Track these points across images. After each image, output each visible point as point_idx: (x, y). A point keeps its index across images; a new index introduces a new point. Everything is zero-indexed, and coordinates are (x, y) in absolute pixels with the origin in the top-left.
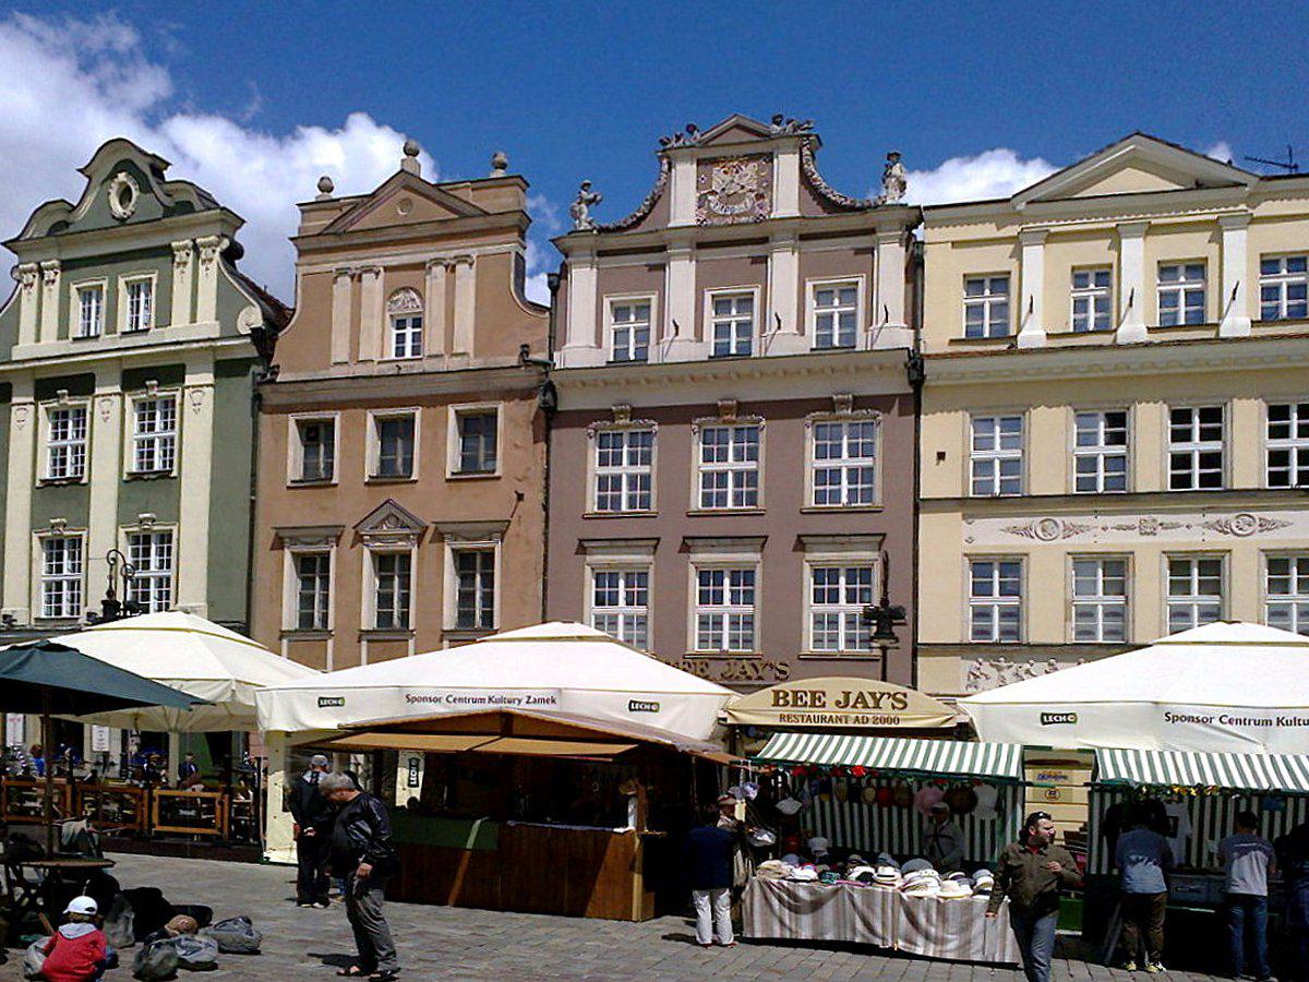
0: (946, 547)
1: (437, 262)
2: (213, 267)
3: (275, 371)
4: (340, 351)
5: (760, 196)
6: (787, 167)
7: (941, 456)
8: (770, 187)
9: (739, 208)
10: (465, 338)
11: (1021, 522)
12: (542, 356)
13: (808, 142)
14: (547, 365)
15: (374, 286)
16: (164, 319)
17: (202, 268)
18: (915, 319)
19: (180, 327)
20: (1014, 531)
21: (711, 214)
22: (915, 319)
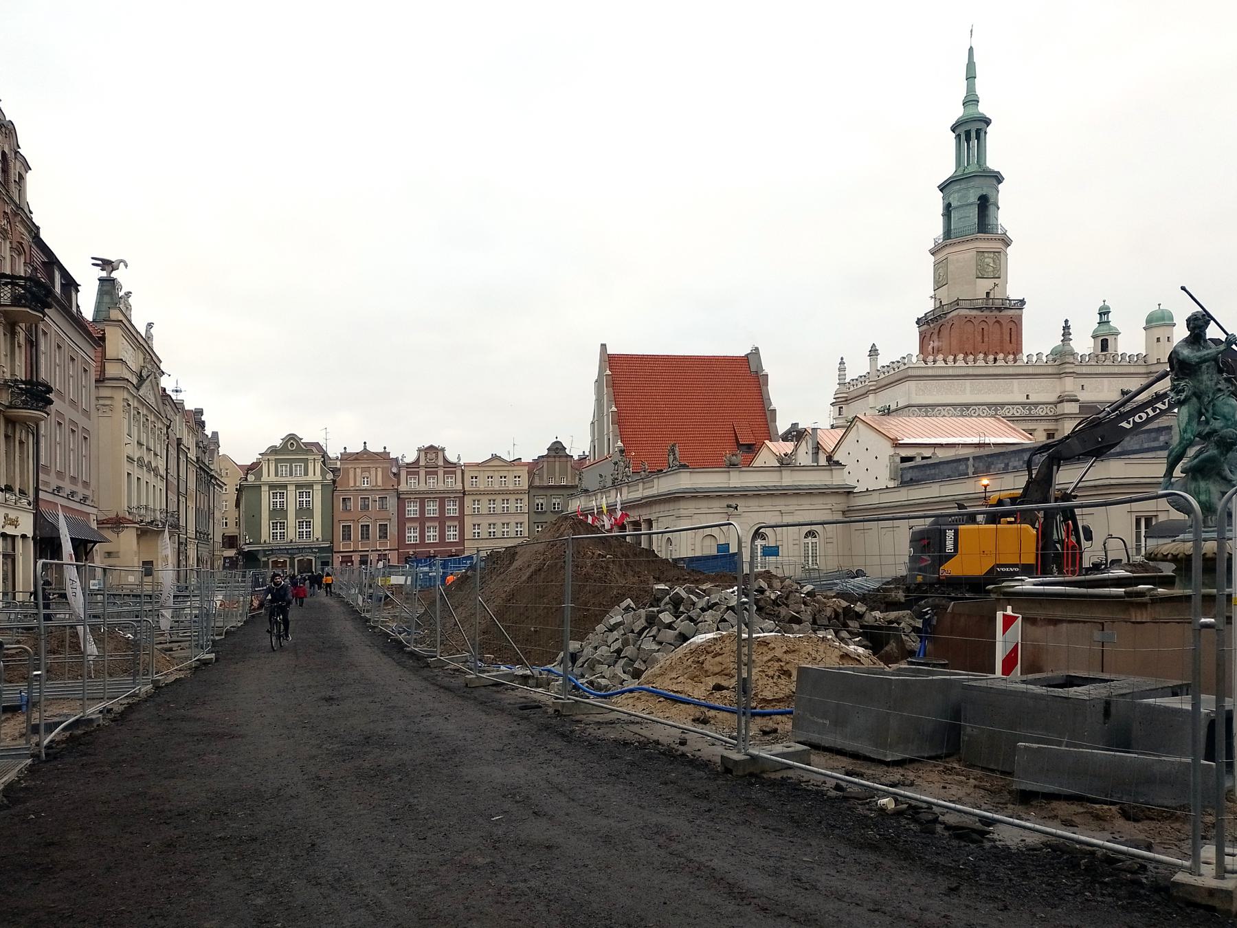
6: (440, 454)
10: (380, 483)
16: (306, 474)
19: (311, 477)
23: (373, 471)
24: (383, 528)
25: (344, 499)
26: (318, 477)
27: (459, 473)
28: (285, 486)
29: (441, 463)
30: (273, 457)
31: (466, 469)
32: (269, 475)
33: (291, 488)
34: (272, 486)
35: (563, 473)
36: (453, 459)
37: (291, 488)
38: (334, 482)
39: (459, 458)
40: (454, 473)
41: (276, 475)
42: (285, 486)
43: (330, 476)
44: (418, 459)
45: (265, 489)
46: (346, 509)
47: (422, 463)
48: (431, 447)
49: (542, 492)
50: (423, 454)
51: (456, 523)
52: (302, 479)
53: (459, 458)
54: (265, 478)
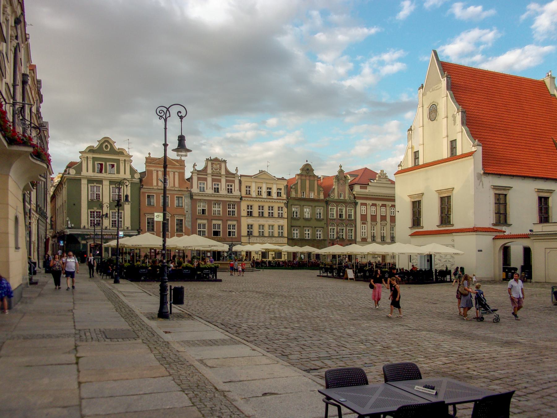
0: (245, 222)
16: (118, 172)
17: (126, 164)
18: (240, 191)
19: (122, 175)
22: (240, 191)
24: (180, 222)
25: (149, 196)
26: (128, 176)
27: (237, 182)
28: (100, 182)
29: (223, 172)
30: (90, 156)
31: (243, 179)
32: (88, 172)
33: (106, 183)
34: (90, 181)
35: (311, 189)
36: (232, 170)
37: (106, 183)
38: (141, 180)
39: (237, 170)
40: (233, 182)
41: (94, 171)
42: (100, 182)
43: (137, 176)
44: (206, 168)
45: (84, 182)
46: (149, 204)
47: (209, 171)
48: (216, 160)
49: (296, 202)
50: (209, 163)
51: (235, 223)
52: (115, 176)
53: (237, 170)
54: (84, 173)
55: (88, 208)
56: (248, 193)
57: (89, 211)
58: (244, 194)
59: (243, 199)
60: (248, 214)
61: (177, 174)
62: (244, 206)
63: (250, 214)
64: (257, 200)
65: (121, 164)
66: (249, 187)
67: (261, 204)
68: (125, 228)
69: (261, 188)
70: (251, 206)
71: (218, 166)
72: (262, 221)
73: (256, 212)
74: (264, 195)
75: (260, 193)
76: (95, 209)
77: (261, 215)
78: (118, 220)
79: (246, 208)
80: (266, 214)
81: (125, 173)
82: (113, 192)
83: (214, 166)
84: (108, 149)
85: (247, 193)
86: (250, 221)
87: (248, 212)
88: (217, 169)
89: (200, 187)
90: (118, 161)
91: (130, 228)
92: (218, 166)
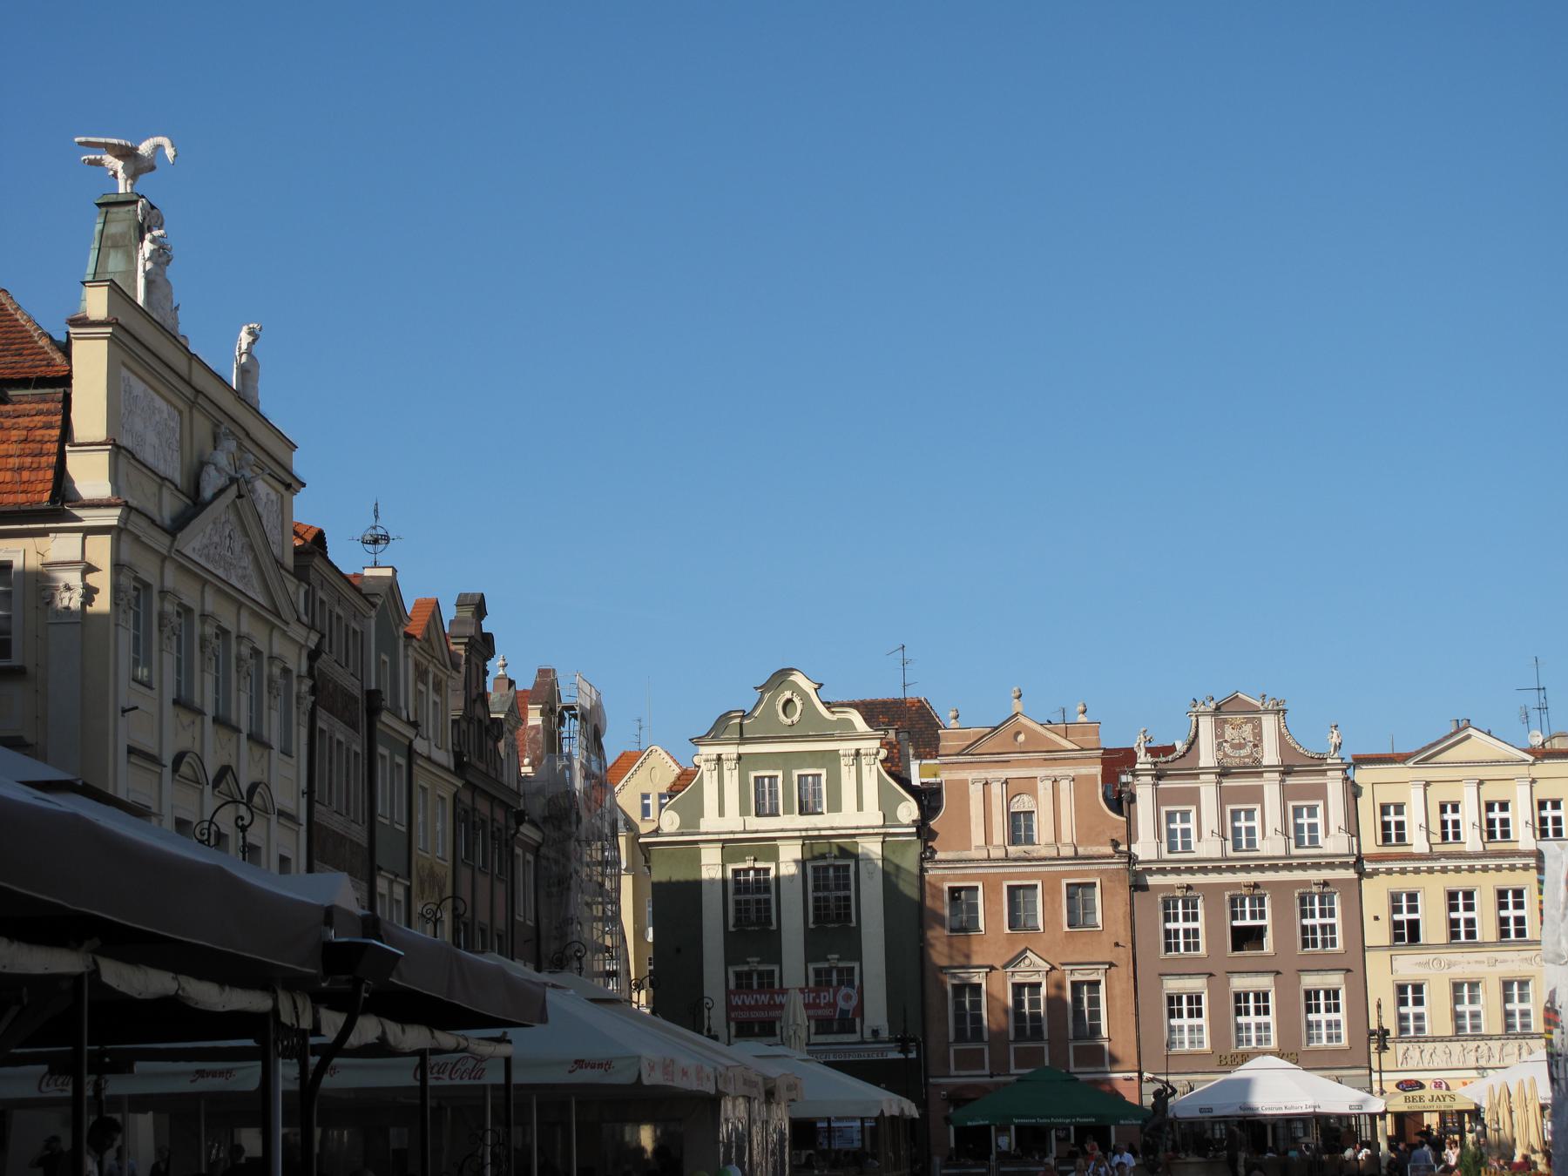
1: (1047, 778)
2: (874, 768)
3: (934, 852)
4: (977, 837)
5: (1255, 746)
6: (1269, 724)
7: (1376, 918)
8: (1261, 740)
9: (1243, 752)
10: (1067, 834)
11: (1424, 958)
12: (1123, 848)
13: (1280, 712)
14: (1131, 858)
15: (996, 789)
16: (835, 806)
17: (865, 769)
20: (1420, 964)
21: (1226, 755)
23: (1044, 789)
41: (744, 812)
51: (1335, 980)
54: (710, 822)
55: (728, 963)
56: (1392, 833)
57: (731, 970)
58: (1370, 843)
59: (1368, 867)
60: (1398, 937)
61: (1064, 785)
62: (1375, 895)
63: (1407, 934)
64: (1437, 865)
65: (844, 770)
66: (1399, 809)
67: (1460, 882)
68: (868, 1035)
69: (1455, 809)
70: (1412, 897)
71: (1248, 728)
72: (1465, 964)
73: (1433, 925)
74: (1472, 839)
75: (1451, 831)
76: (754, 964)
77: (1460, 934)
78: (508, 1125)
79: (1384, 909)
80: (1487, 929)
81: (860, 808)
82: (816, 888)
83: (1229, 733)
84: (796, 718)
85: (1386, 838)
86: (1409, 965)
87: (1397, 925)
88: (1241, 746)
89: (1172, 834)
90: (831, 759)
91: (885, 1034)
92: (1248, 728)
